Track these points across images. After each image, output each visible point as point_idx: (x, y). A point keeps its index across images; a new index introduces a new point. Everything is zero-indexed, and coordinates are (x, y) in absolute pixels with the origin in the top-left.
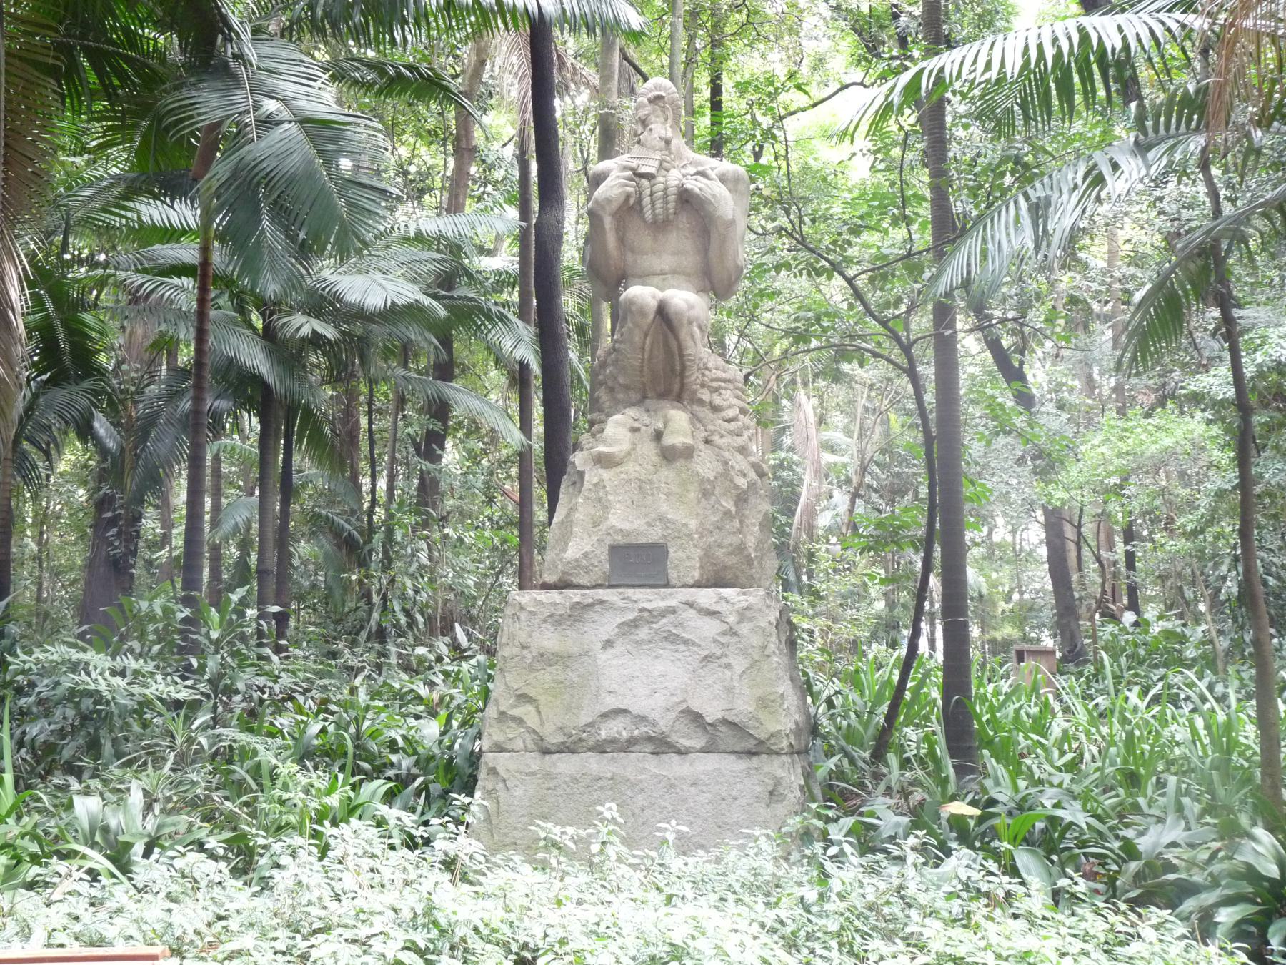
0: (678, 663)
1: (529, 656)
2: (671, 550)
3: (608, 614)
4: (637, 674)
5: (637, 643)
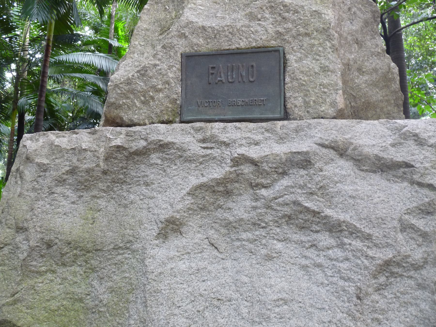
0: (319, 276)
1: (24, 247)
2: (291, 58)
3: (172, 170)
4: (228, 293)
5: (228, 225)
